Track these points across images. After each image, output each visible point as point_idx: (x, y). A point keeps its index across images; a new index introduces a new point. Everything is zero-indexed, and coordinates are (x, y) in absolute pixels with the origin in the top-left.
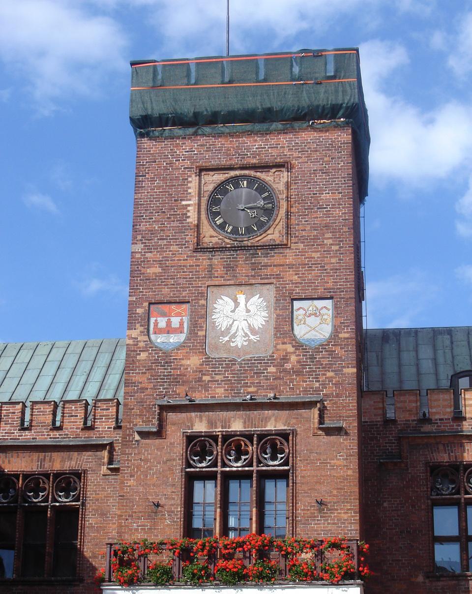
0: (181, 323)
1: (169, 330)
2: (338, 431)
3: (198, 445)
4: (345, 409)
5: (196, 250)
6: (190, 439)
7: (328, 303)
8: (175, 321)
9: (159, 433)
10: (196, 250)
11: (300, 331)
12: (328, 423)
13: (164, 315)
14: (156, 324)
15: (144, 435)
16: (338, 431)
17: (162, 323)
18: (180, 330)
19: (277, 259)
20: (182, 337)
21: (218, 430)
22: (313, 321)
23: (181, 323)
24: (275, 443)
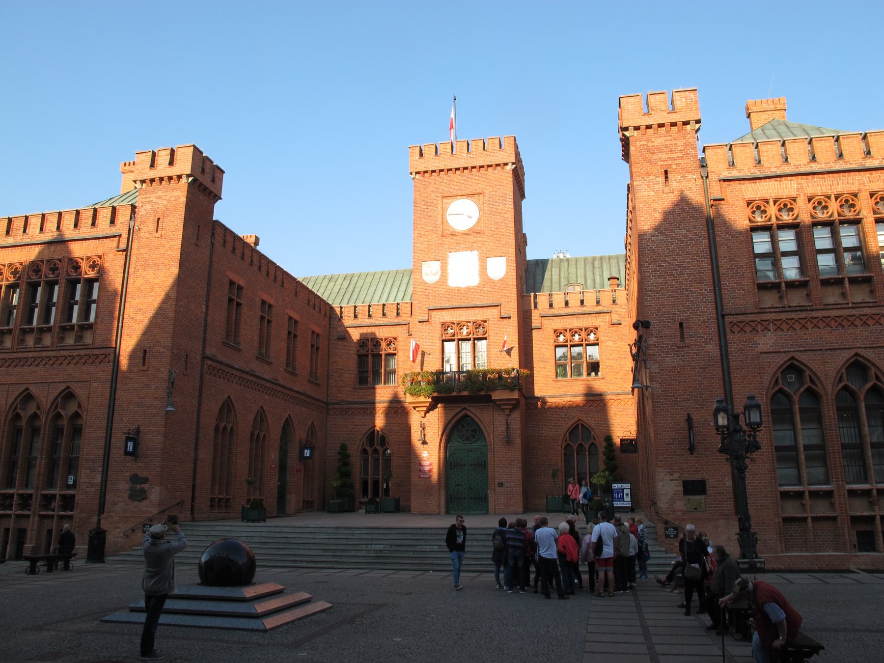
3: (445, 326)
10: (443, 235)
12: (503, 315)
19: (480, 239)
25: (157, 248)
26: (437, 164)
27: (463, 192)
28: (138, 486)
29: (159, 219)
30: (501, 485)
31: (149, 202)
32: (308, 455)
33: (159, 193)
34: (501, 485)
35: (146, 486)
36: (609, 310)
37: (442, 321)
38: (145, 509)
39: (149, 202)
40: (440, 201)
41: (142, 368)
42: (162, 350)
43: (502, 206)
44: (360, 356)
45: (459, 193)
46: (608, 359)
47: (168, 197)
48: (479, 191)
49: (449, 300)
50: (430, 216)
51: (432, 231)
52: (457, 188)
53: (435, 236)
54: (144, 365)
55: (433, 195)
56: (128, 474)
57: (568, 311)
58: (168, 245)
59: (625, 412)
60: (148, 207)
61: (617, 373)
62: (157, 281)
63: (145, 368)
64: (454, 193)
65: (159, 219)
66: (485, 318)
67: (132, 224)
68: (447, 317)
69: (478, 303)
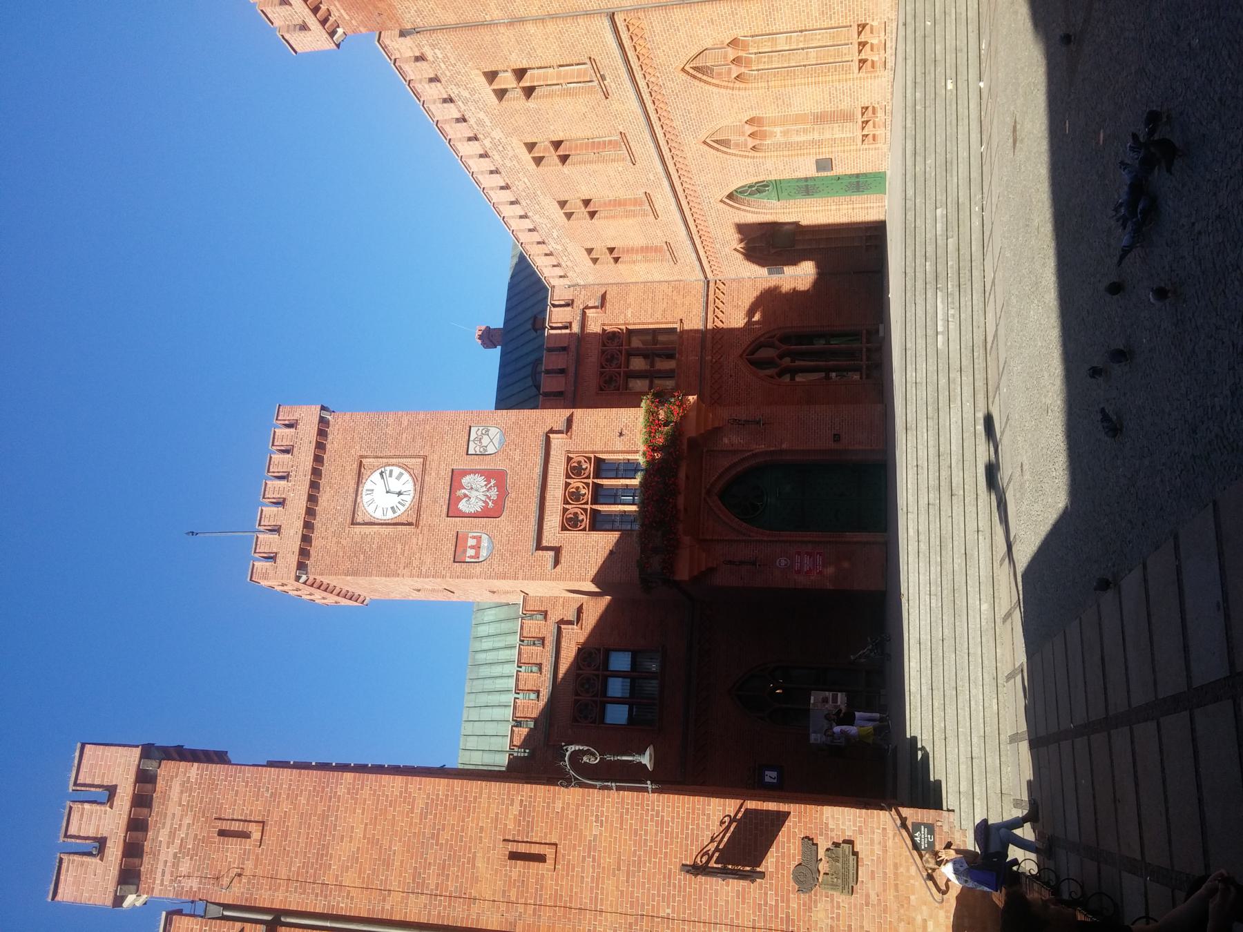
0: (474, 537)
1: (477, 547)
2: (570, 421)
3: (570, 523)
4: (555, 417)
5: (417, 526)
6: (564, 528)
7: (473, 430)
8: (471, 542)
9: (557, 550)
10: (417, 526)
11: (491, 450)
12: (564, 428)
13: (465, 552)
14: (471, 557)
15: (557, 562)
16: (570, 421)
17: (471, 552)
18: (479, 539)
19: (434, 465)
20: (484, 537)
21: (560, 507)
22: (485, 440)
23: (474, 537)
24: (574, 470)
25: (285, 835)
26: (292, 532)
27: (352, 490)
28: (823, 867)
29: (222, 833)
30: (837, 438)
31: (175, 865)
32: (774, 774)
33: (163, 836)
34: (837, 438)
35: (823, 844)
36: (579, 312)
37: (558, 529)
38: (877, 850)
39: (175, 865)
40: (357, 529)
41: (550, 863)
42: (515, 809)
43: (389, 431)
44: (593, 527)
45: (351, 498)
46: (652, 315)
47: (178, 811)
48: (355, 466)
49: (527, 517)
50: (379, 547)
51: (404, 545)
52: (341, 501)
53: (414, 541)
54: (541, 858)
55: (344, 542)
56: (796, 901)
57: (572, 370)
58: (286, 806)
59: (735, 294)
60: (185, 867)
61: (675, 303)
62: (359, 831)
63: (548, 851)
64: (349, 505)
65: (222, 833)
66: (564, 460)
67: (214, 911)
68: (553, 520)
69: (538, 470)
